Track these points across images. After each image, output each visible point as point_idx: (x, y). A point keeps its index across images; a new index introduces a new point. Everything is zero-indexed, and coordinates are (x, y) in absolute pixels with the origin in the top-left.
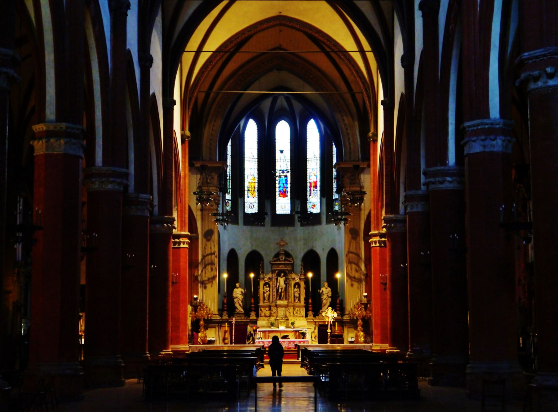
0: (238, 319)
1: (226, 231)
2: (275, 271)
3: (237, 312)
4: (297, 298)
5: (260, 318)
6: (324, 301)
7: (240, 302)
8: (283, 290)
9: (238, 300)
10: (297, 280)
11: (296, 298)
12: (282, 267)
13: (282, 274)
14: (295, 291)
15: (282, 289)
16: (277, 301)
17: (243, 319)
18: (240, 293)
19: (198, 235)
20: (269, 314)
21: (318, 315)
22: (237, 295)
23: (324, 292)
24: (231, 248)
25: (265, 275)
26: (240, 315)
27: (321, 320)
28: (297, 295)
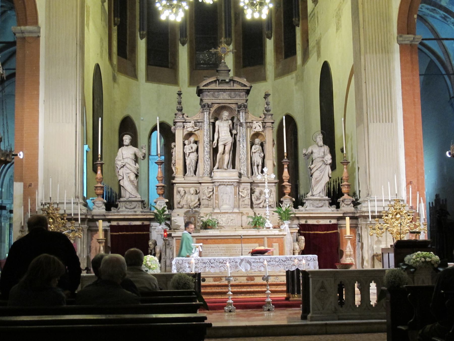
0: (130, 213)
1: (116, 85)
2: (209, 106)
3: (125, 199)
4: (258, 166)
5: (175, 211)
6: (316, 174)
7: (133, 177)
8: (228, 148)
9: (129, 171)
10: (257, 126)
11: (255, 167)
12: (224, 98)
13: (225, 114)
14: (253, 150)
15: (225, 145)
16: (213, 172)
17: (138, 213)
18: (133, 157)
19: (39, 28)
20: (197, 200)
21: (302, 204)
22: (126, 160)
23: (315, 156)
24: (125, 114)
25: (187, 117)
26: (134, 204)
27: (311, 215)
28: (257, 159)
